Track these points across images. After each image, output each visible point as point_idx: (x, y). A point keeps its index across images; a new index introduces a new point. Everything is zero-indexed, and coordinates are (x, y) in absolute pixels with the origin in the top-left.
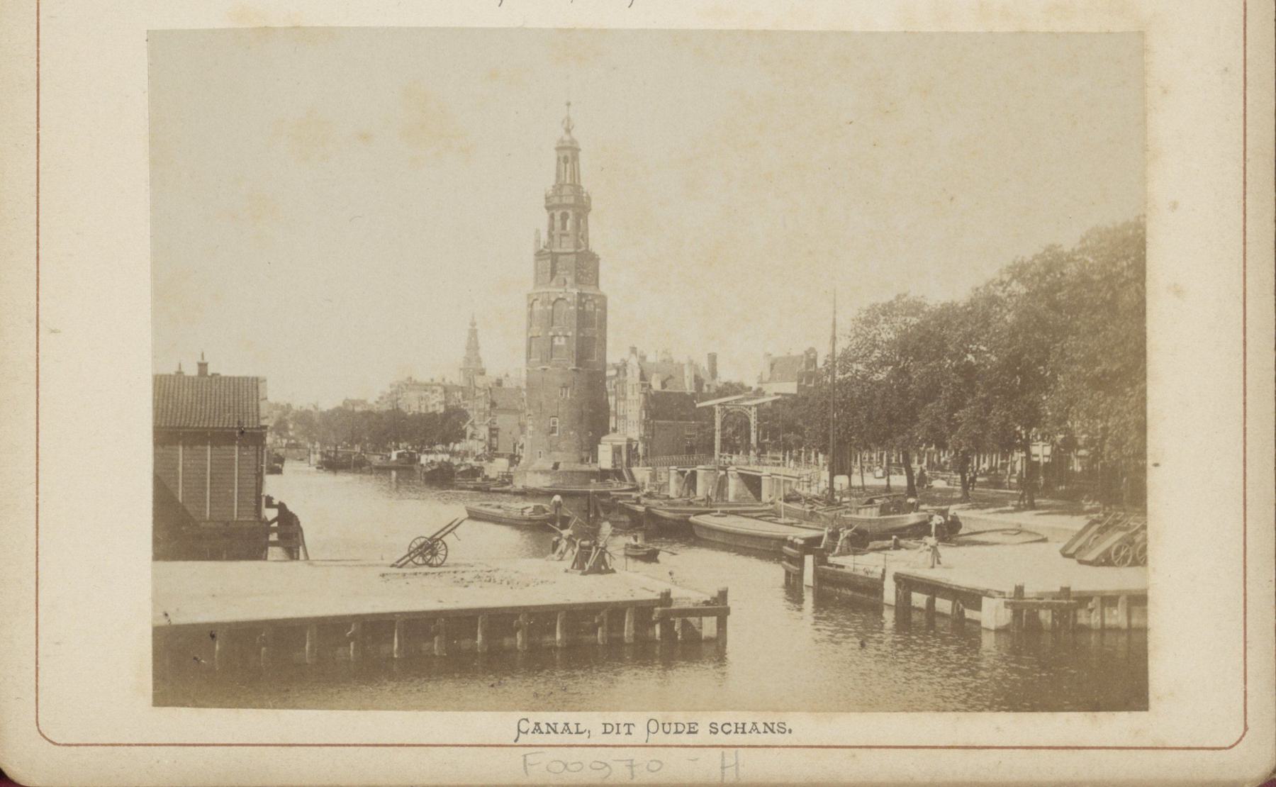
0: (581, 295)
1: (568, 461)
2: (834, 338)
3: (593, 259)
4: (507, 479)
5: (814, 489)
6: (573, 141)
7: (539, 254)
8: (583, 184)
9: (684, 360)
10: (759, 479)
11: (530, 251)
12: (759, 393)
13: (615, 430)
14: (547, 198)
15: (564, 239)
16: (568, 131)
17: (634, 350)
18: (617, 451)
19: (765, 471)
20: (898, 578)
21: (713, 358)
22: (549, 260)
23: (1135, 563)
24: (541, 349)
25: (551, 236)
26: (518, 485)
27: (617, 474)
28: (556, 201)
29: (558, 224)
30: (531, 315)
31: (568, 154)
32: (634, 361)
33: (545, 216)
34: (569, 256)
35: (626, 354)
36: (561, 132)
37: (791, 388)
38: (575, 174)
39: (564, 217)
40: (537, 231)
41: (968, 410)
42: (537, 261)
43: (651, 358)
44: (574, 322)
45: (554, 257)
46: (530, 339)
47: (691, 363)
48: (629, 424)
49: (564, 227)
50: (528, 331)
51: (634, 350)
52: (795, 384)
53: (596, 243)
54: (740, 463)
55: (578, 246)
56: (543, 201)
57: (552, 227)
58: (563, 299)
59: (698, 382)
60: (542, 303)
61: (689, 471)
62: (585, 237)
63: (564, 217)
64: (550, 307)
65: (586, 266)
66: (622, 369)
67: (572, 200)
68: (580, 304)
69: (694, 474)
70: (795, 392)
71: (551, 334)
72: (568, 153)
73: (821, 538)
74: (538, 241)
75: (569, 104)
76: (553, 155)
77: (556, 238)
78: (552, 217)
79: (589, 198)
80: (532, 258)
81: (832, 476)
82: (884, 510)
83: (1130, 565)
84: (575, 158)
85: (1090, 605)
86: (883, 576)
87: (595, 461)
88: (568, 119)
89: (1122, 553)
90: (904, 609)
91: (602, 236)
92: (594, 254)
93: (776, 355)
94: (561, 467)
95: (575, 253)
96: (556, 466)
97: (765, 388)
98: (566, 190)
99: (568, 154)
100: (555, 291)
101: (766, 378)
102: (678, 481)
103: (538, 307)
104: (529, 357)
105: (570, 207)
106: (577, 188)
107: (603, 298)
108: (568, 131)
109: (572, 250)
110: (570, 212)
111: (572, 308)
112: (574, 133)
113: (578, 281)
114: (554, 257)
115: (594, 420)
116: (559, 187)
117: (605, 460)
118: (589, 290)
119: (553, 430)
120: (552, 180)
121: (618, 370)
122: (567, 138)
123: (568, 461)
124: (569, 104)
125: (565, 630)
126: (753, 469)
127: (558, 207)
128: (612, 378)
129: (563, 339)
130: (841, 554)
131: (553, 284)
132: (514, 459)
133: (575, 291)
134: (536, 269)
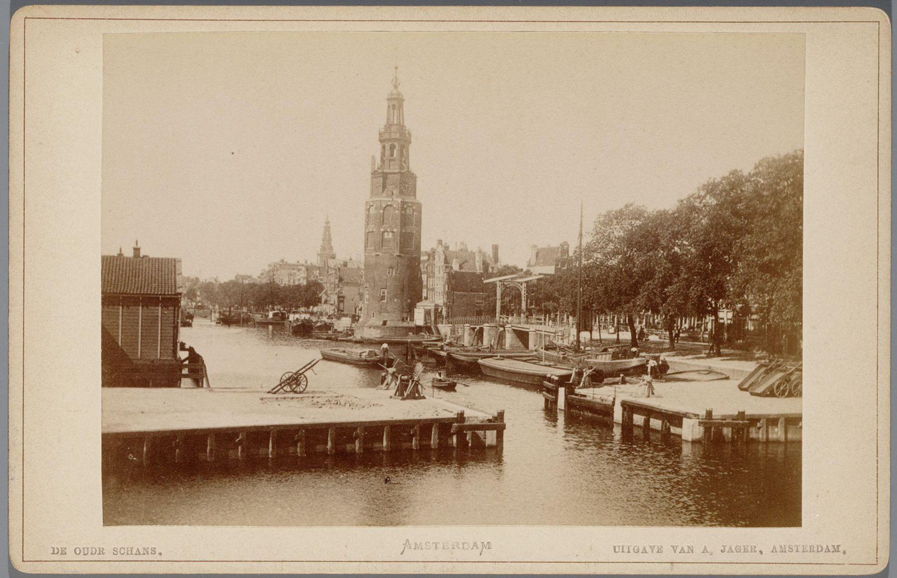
0: (403, 203)
1: (394, 320)
2: (581, 235)
3: (414, 178)
4: (350, 332)
5: (566, 341)
6: (399, 94)
7: (374, 174)
9: (475, 250)
10: (527, 333)
11: (369, 170)
12: (528, 273)
13: (426, 298)
14: (380, 134)
15: (392, 163)
16: (396, 87)
17: (440, 242)
18: (427, 313)
19: (531, 328)
20: (624, 404)
21: (496, 248)
22: (382, 179)
23: (790, 395)
24: (375, 241)
25: (383, 161)
26: (358, 336)
27: (428, 329)
28: (386, 136)
29: (388, 153)
30: (368, 216)
31: (396, 103)
32: (440, 250)
33: (379, 146)
34: (394, 175)
35: (434, 245)
36: (393, 88)
37: (550, 270)
38: (401, 116)
39: (392, 148)
40: (373, 157)
41: (674, 286)
42: (372, 178)
43: (450, 249)
44: (398, 222)
45: (385, 176)
46: (367, 234)
47: (480, 252)
48: (436, 293)
49: (392, 155)
50: (366, 228)
51: (440, 242)
52: (553, 268)
53: (415, 165)
54: (514, 322)
55: (401, 167)
57: (383, 154)
58: (391, 206)
59: (485, 265)
60: (376, 209)
61: (478, 327)
62: (406, 161)
63: (392, 148)
64: (382, 211)
65: (406, 183)
66: (432, 255)
67: (398, 136)
68: (403, 209)
69: (481, 330)
70: (553, 273)
71: (382, 230)
72: (395, 102)
73: (571, 375)
74: (374, 163)
75: (396, 68)
76: (385, 104)
77: (387, 162)
78: (384, 147)
79: (410, 134)
80: (369, 176)
81: (579, 332)
82: (615, 356)
83: (787, 396)
84: (401, 106)
85: (759, 425)
86: (614, 403)
87: (412, 320)
88: (396, 78)
89: (782, 388)
90: (627, 426)
91: (418, 161)
92: (413, 174)
93: (540, 246)
94: (388, 323)
95: (400, 173)
96: (385, 323)
97: (532, 269)
98: (394, 128)
99: (396, 103)
100: (385, 199)
101: (532, 263)
102: (470, 335)
103: (373, 211)
104: (366, 247)
105: (396, 142)
106: (401, 127)
107: (419, 206)
108: (396, 87)
109: (397, 171)
110: (396, 144)
111: (397, 212)
112: (399, 88)
113: (401, 192)
114: (385, 176)
115: (411, 290)
116: (389, 126)
117: (419, 319)
118: (408, 200)
119: (383, 298)
120: (383, 122)
121: (429, 256)
122: (395, 92)
123: (394, 320)
125: (391, 439)
126: (523, 327)
127: (389, 140)
128: (424, 261)
129: (390, 234)
130: (584, 387)
131: (384, 194)
132: (355, 318)
133: (399, 200)
134: (372, 184)
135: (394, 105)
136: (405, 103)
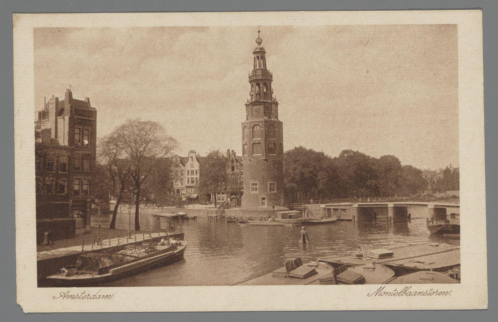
8: (268, 69)
16: (259, 43)
31: (260, 54)
36: (257, 45)
39: (258, 85)
56: (248, 79)
64: (251, 130)
75: (259, 32)
78: (252, 86)
79: (271, 76)
84: (263, 58)
99: (260, 54)
107: (280, 124)
108: (259, 43)
116: (255, 71)
124: (259, 32)
127: (255, 81)
135: (258, 57)
136: (266, 55)
